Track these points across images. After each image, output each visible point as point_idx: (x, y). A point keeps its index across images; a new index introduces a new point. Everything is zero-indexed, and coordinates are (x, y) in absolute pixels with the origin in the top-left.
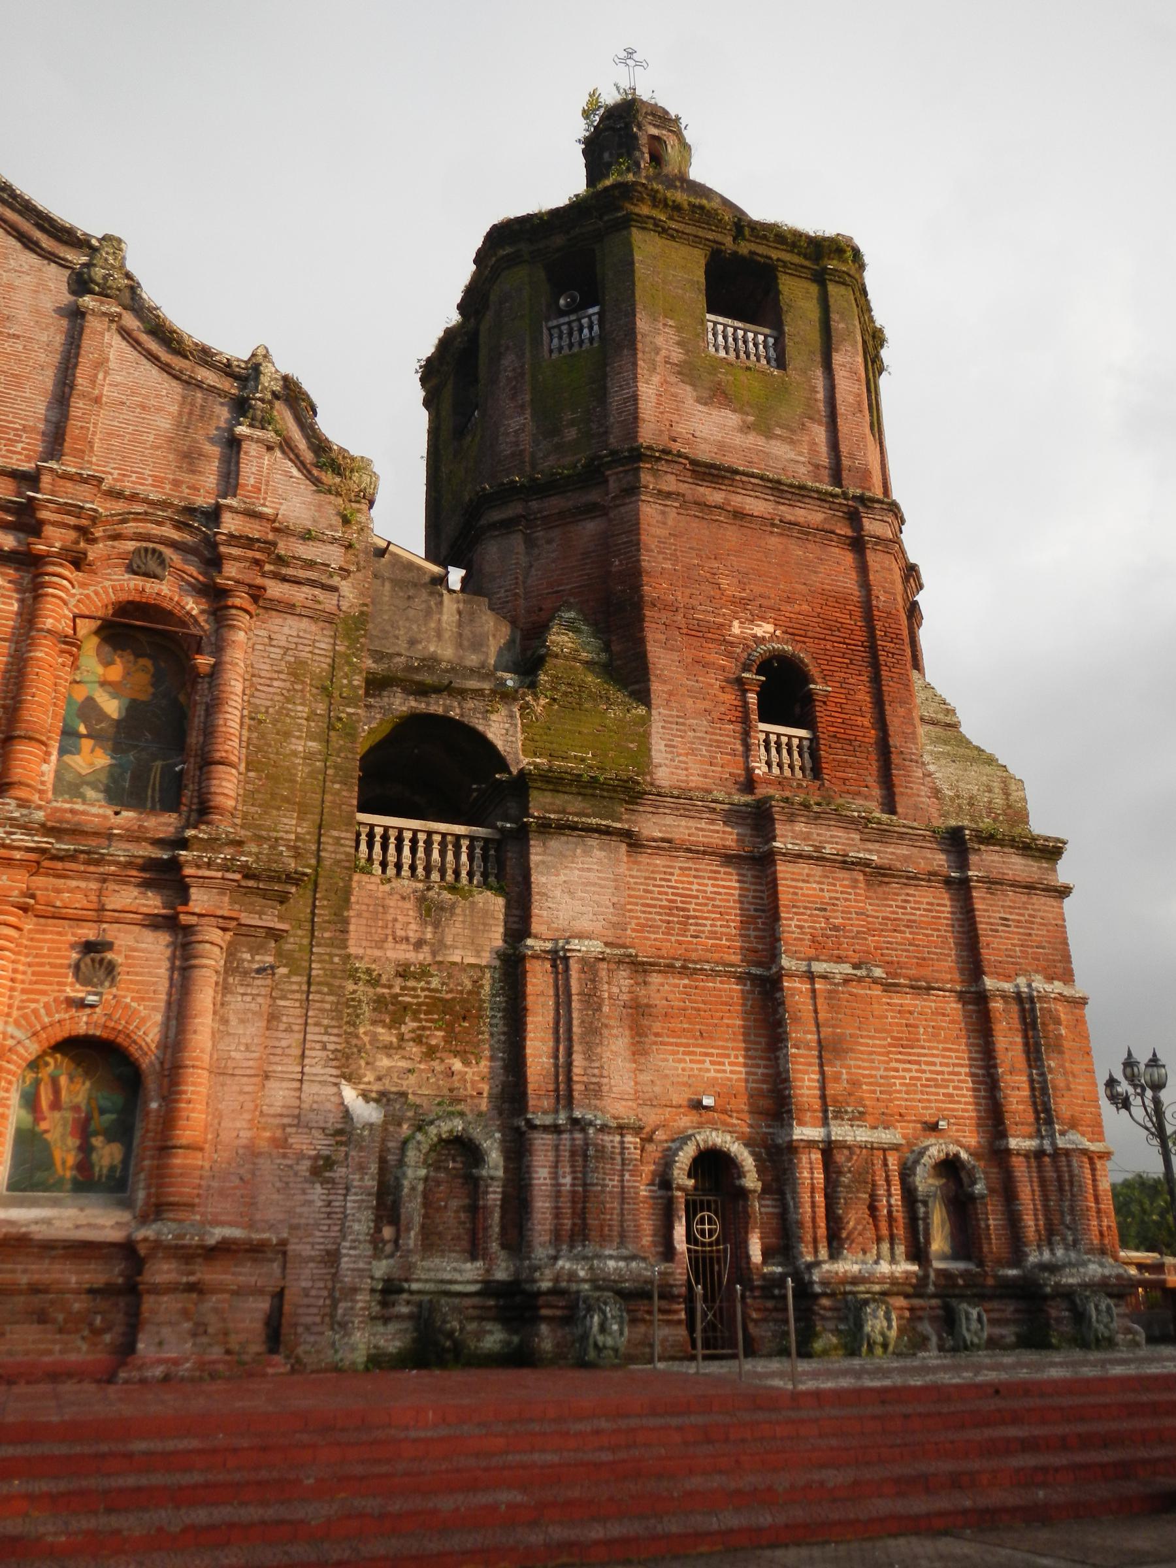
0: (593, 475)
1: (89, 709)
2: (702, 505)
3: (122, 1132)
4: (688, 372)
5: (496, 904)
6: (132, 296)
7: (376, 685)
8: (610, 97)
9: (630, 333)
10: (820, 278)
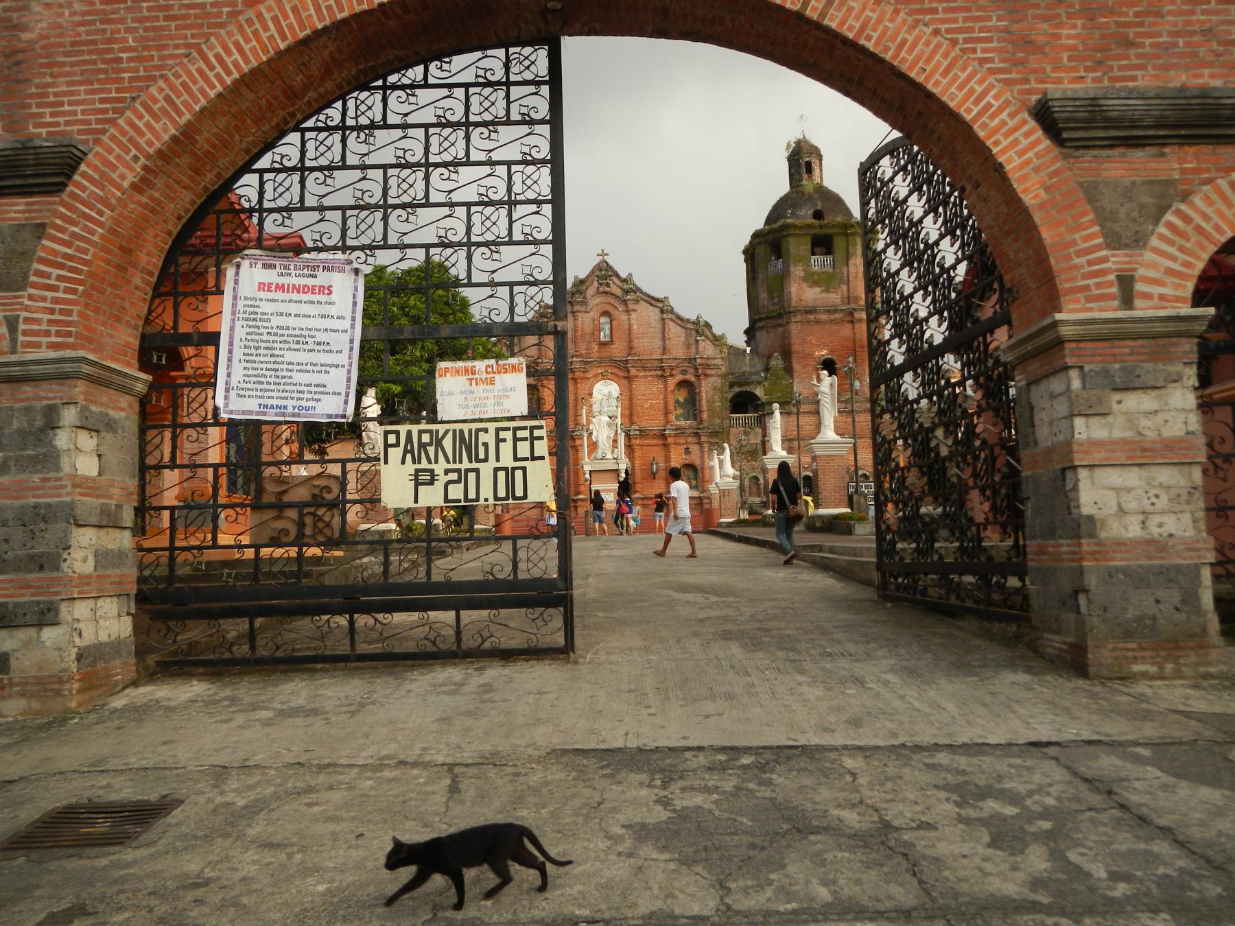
0: (780, 316)
1: (677, 401)
2: (809, 322)
3: (696, 479)
4: (805, 279)
5: (760, 430)
6: (672, 311)
7: (732, 385)
8: (793, 140)
9: (789, 272)
10: (847, 235)
